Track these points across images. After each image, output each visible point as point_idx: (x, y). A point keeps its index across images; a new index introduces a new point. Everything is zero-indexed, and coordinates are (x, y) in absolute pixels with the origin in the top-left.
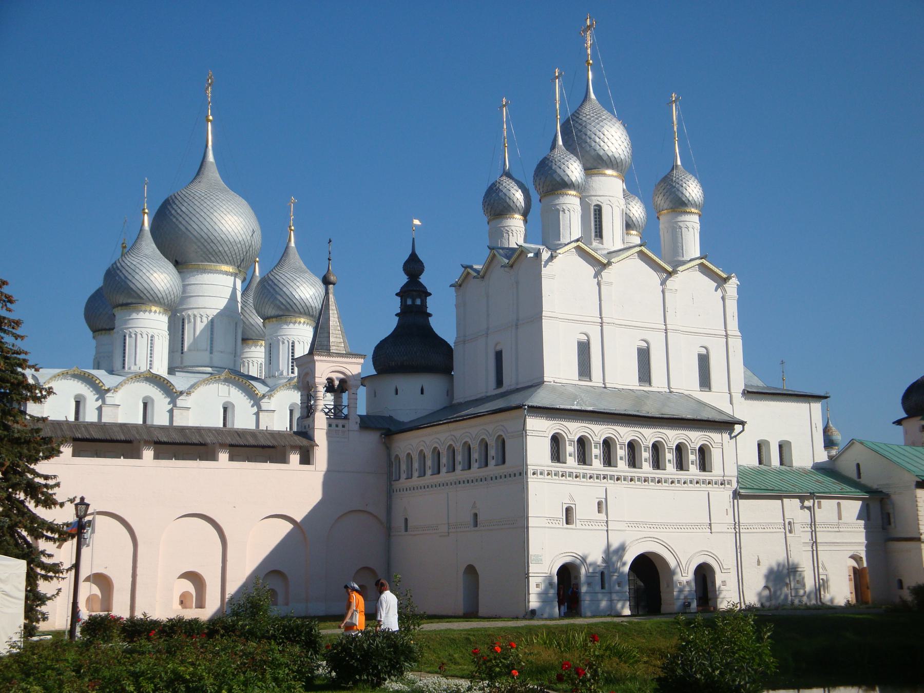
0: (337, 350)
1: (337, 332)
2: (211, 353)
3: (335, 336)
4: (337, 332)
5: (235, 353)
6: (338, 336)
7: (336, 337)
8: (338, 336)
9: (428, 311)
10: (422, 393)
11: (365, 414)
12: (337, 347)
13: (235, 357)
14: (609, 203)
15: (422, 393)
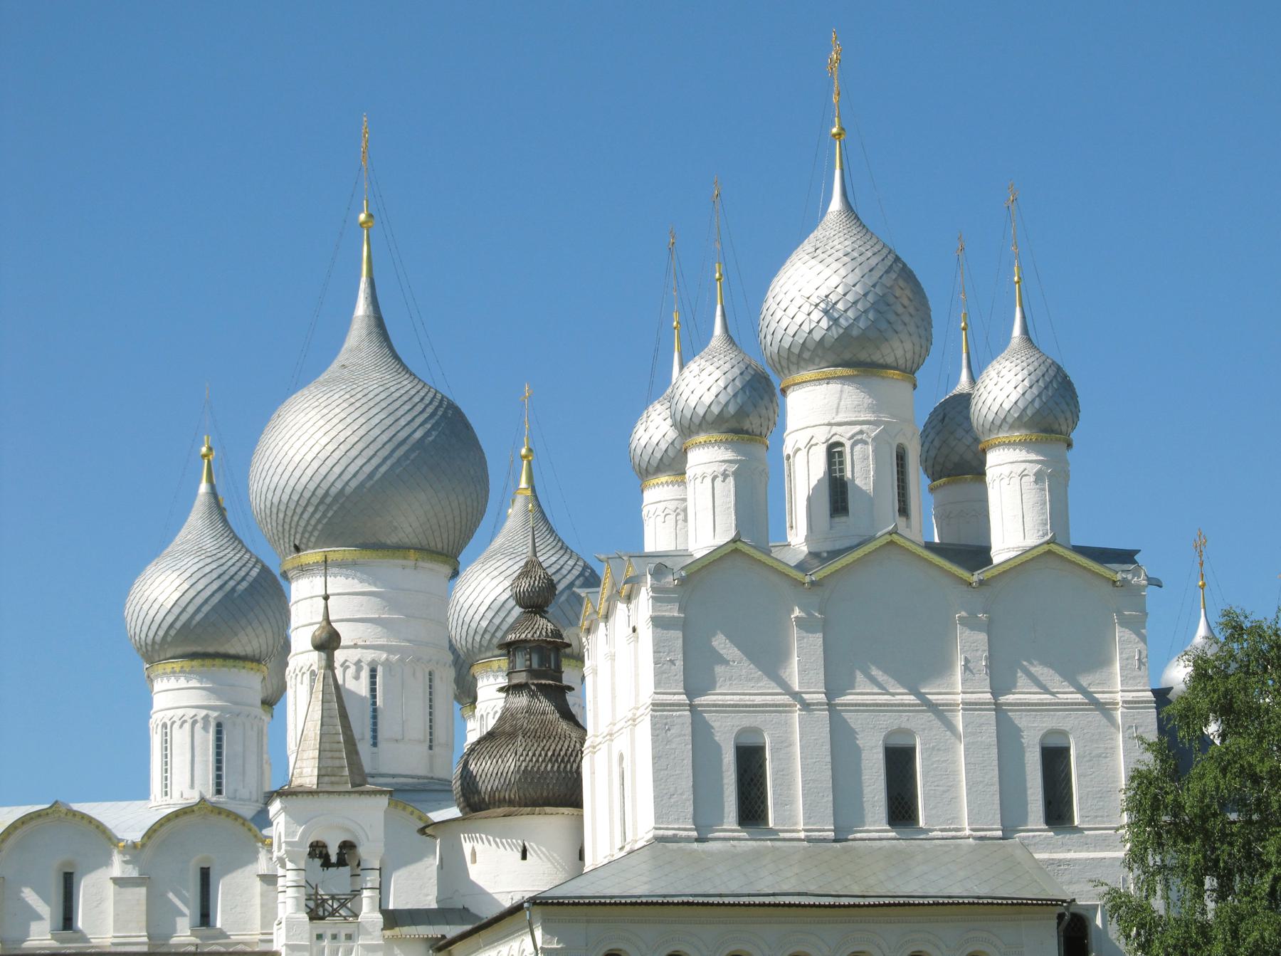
0: (332, 783)
1: (335, 746)
2: (375, 745)
3: (329, 754)
4: (335, 746)
5: (431, 741)
6: (337, 754)
7: (332, 758)
8: (337, 754)
9: (565, 682)
10: (524, 857)
11: (434, 906)
12: (333, 779)
13: (431, 748)
14: (859, 437)
15: (524, 857)
